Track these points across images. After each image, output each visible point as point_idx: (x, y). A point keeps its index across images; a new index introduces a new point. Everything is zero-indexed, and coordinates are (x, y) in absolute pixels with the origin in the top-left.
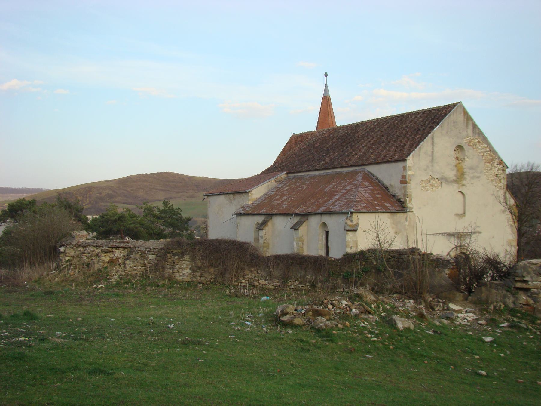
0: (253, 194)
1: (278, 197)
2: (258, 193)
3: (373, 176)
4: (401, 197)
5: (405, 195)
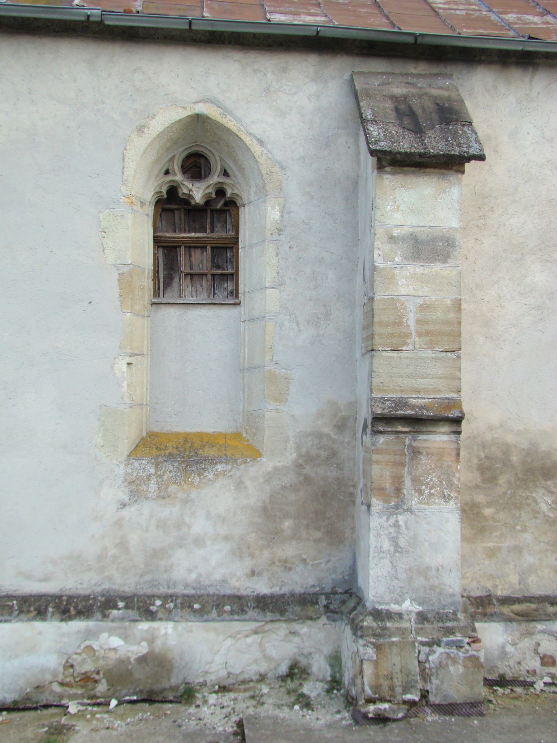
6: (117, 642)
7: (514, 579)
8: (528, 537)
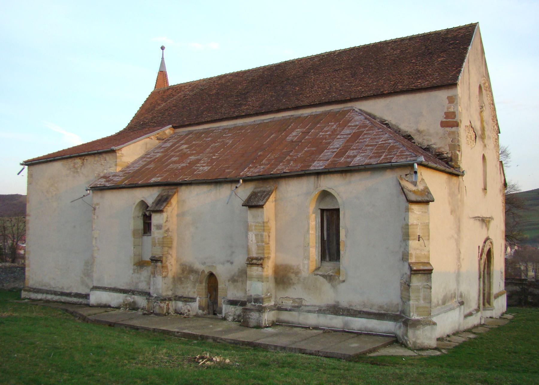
0: (122, 156)
1: (174, 159)
2: (131, 153)
3: (374, 117)
4: (446, 150)
5: (455, 146)
6: (130, 298)
7: (187, 293)
8: (189, 285)
